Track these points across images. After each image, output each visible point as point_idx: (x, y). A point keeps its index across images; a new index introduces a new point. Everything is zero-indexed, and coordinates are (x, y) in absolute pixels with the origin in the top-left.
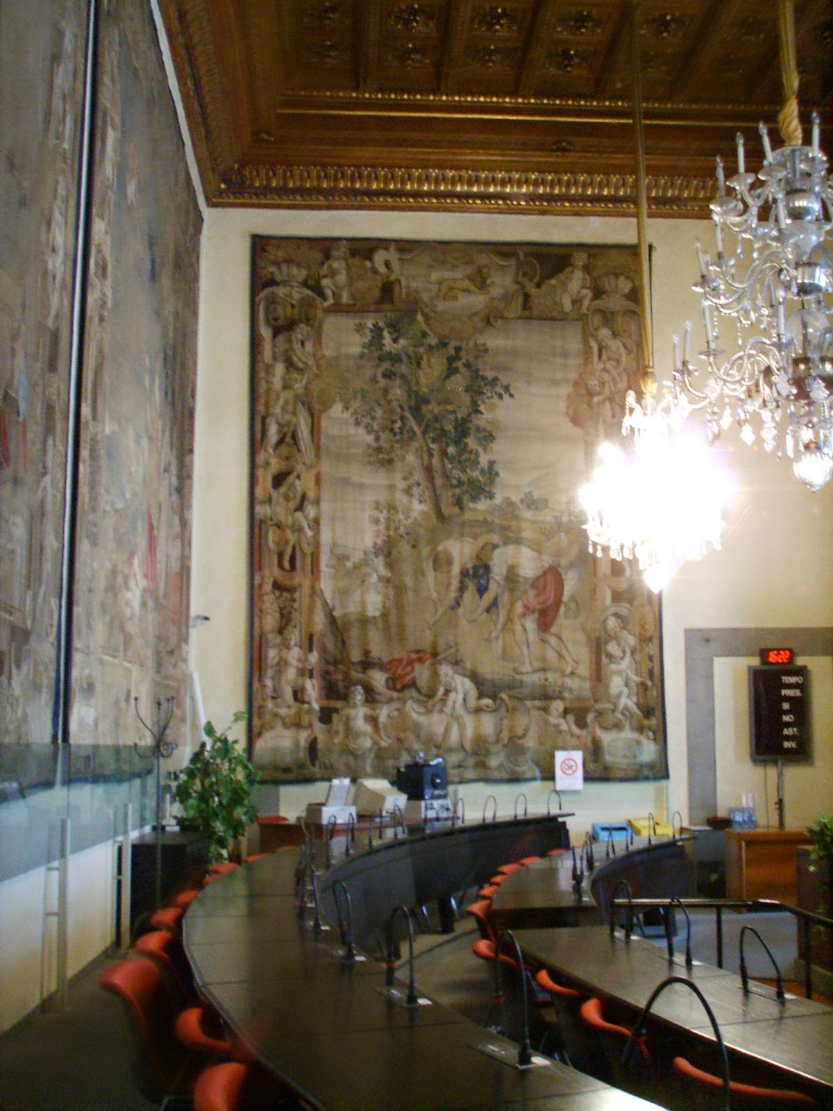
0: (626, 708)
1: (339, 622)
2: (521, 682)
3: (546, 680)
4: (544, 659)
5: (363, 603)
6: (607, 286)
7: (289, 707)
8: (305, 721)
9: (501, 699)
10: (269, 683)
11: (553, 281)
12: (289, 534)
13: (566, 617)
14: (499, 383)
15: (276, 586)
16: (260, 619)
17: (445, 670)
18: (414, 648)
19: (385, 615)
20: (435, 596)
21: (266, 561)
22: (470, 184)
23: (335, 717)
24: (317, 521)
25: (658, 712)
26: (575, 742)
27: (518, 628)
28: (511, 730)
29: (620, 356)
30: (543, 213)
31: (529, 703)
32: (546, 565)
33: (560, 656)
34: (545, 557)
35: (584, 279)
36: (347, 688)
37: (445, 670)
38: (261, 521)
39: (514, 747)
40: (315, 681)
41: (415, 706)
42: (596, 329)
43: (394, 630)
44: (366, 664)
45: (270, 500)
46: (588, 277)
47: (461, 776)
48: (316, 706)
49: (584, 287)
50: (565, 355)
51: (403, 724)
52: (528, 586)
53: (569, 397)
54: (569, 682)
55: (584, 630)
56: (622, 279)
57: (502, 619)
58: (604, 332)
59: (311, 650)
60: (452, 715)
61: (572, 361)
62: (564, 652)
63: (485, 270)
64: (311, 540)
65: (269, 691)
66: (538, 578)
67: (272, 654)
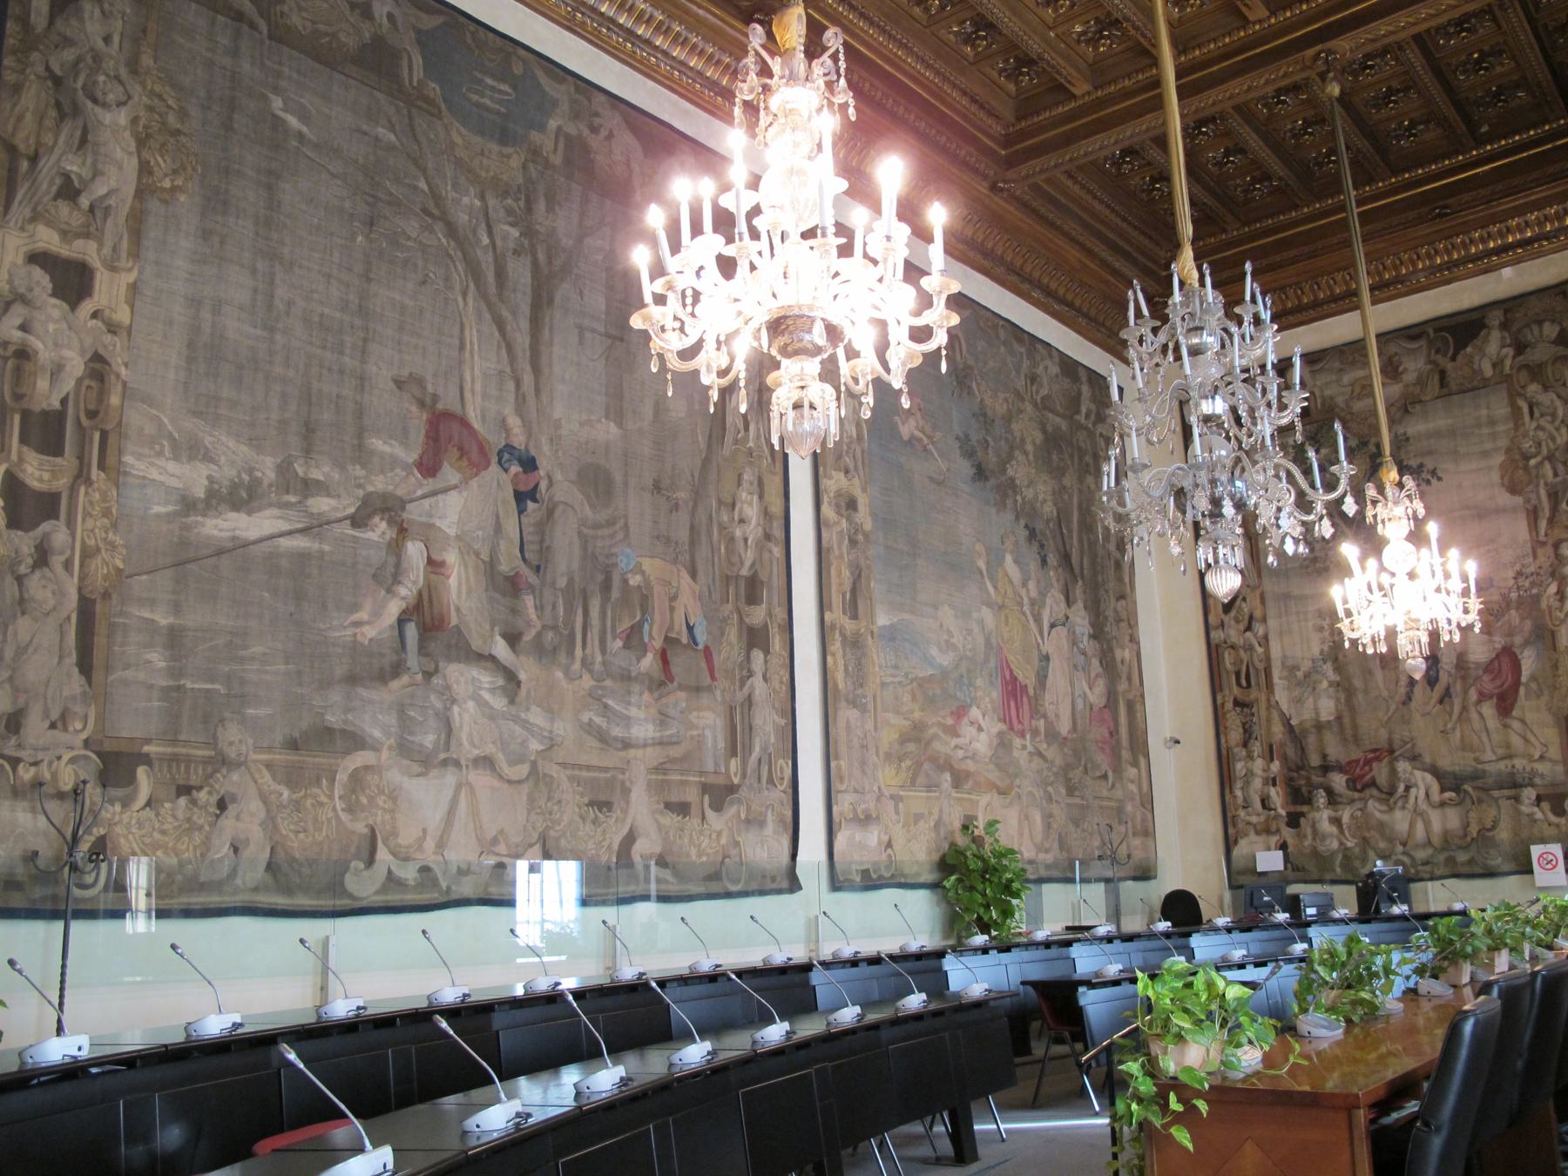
1: (1297, 731)
2: (1484, 771)
3: (1513, 767)
4: (1508, 746)
5: (1316, 710)
6: (1529, 337)
7: (1259, 815)
8: (1274, 828)
9: (1465, 791)
10: (1239, 793)
11: (1469, 350)
12: (1242, 652)
13: (1527, 697)
14: (1425, 469)
15: (1237, 703)
16: (1226, 735)
17: (1403, 766)
18: (1369, 748)
19: (1339, 718)
20: (1385, 693)
21: (1225, 682)
22: (1521, 231)
23: (1302, 820)
24: (1266, 638)
26: (1552, 831)
27: (1474, 716)
28: (1480, 821)
29: (1555, 409)
30: (1448, 282)
31: (1496, 793)
32: (1498, 646)
33: (1526, 740)
34: (1497, 638)
35: (1503, 338)
36: (1310, 792)
37: (1403, 766)
38: (1217, 646)
39: (1484, 838)
40: (1278, 788)
41: (1377, 805)
42: (1523, 387)
43: (1349, 732)
44: (1326, 768)
45: (1222, 625)
46: (1507, 335)
47: (1432, 873)
48: (1283, 812)
49: (1503, 346)
50: (1492, 422)
51: (1363, 826)
52: (1481, 672)
53: (1502, 466)
54: (1540, 767)
55: (1549, 709)
56: (1547, 327)
57: (1457, 708)
58: (1533, 388)
59: (1272, 760)
60: (1415, 811)
61: (1501, 428)
63: (1396, 359)
64: (1263, 656)
65: (1240, 801)
66: (1492, 661)
67: (1240, 767)
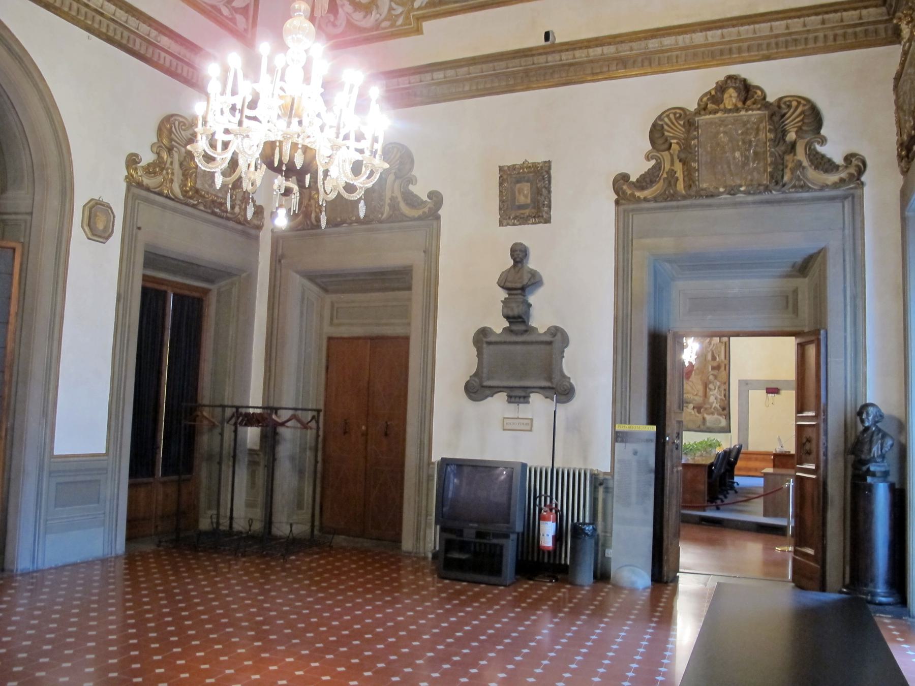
0: (715, 407)
25: (727, 409)
62: (694, 388)
